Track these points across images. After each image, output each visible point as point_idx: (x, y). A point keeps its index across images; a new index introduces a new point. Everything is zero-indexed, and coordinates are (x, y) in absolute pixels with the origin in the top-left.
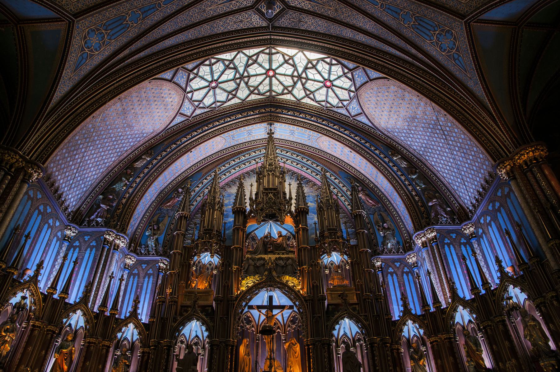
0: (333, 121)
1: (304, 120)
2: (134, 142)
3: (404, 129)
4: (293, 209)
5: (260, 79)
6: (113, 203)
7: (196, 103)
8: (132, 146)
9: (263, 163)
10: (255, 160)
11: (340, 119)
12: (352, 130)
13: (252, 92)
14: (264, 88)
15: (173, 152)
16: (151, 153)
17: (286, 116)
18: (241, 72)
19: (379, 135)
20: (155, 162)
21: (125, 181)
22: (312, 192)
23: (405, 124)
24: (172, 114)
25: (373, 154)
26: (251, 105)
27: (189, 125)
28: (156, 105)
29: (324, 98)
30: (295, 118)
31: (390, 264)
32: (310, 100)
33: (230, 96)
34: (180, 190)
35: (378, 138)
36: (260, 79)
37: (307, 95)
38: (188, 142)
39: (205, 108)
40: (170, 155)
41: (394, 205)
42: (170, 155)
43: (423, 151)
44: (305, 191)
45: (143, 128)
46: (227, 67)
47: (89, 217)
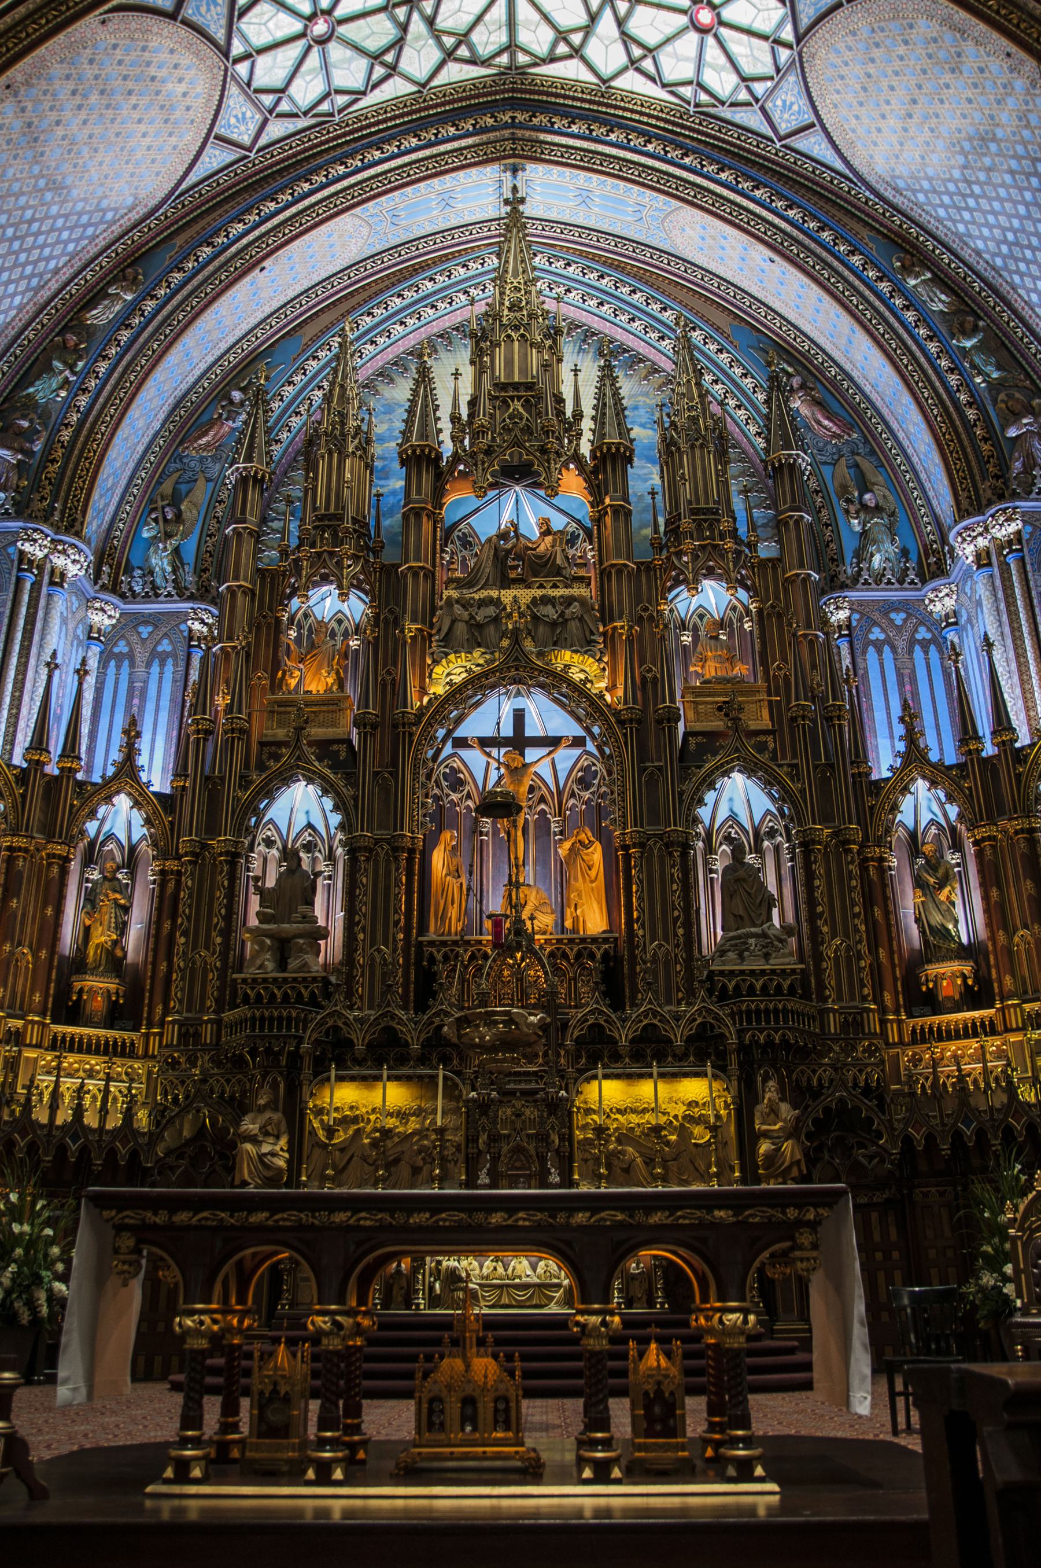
0: (716, 154)
1: (622, 154)
2: (77, 241)
3: (949, 180)
4: (585, 449)
6: (32, 442)
7: (268, 100)
8: (73, 255)
9: (490, 300)
10: (466, 292)
11: (740, 147)
12: (779, 187)
13: (449, 55)
15: (206, 272)
16: (135, 278)
17: (564, 140)
19: (866, 203)
20: (150, 305)
21: (62, 372)
22: (647, 395)
23: (953, 162)
24: (192, 139)
25: (841, 268)
26: (449, 103)
28: (135, 107)
29: (687, 71)
30: (593, 146)
31: (876, 616)
32: (642, 79)
33: (379, 71)
34: (237, 395)
38: (251, 237)
39: (296, 116)
40: (195, 282)
41: (901, 435)
42: (195, 282)
43: (1004, 257)
44: (623, 392)
45: (99, 193)
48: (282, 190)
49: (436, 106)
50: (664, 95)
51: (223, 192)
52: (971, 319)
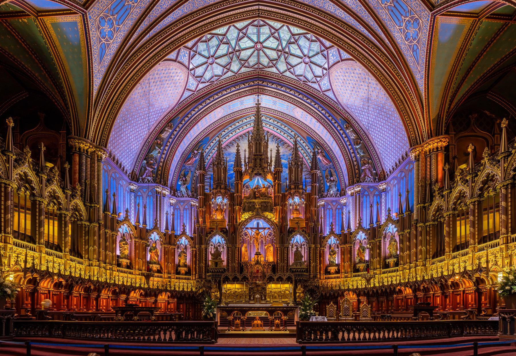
0: (306, 95)
1: (284, 93)
4: (272, 169)
5: (249, 52)
8: (156, 121)
11: (312, 93)
12: (321, 104)
13: (243, 65)
14: (252, 61)
17: (270, 89)
25: (332, 126)
27: (195, 99)
30: (277, 91)
33: (225, 70)
35: (339, 112)
36: (249, 52)
37: (288, 70)
38: (197, 115)
39: (205, 82)
40: (185, 126)
42: (185, 126)
45: (161, 105)
47: (142, 176)
48: (203, 102)
49: (240, 79)
50: (295, 78)
52: (359, 141)
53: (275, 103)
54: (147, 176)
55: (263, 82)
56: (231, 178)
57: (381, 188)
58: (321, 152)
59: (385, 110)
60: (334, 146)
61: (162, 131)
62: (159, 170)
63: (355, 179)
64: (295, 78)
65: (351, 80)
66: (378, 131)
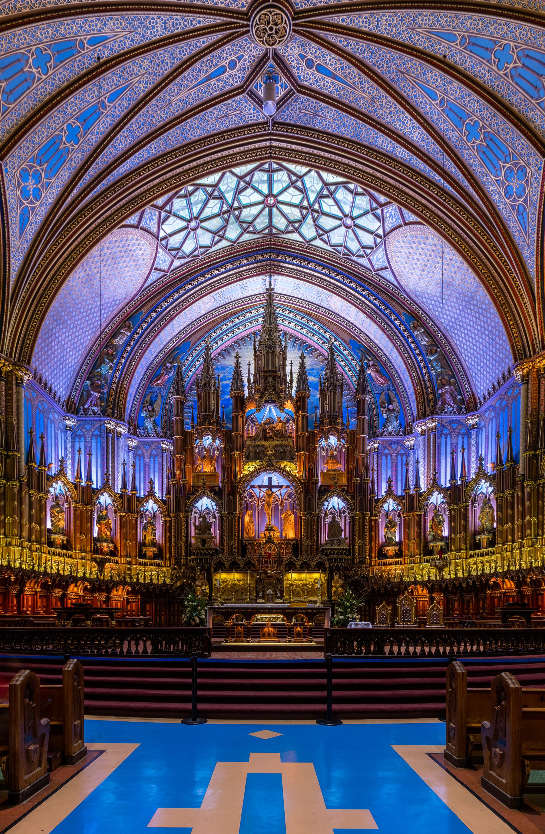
0: (349, 275)
1: (312, 273)
5: (255, 210)
13: (245, 230)
14: (261, 223)
15: (155, 323)
18: (230, 201)
20: (136, 337)
25: (391, 325)
30: (301, 269)
32: (322, 242)
33: (217, 238)
35: (402, 303)
36: (255, 210)
37: (319, 236)
38: (170, 308)
39: (184, 258)
40: (152, 326)
42: (152, 326)
46: (210, 196)
47: (83, 406)
48: (181, 288)
49: (240, 251)
50: (331, 249)
51: (158, 289)
52: (435, 348)
53: (298, 288)
54: (91, 405)
55: (278, 256)
56: (227, 406)
57: (470, 422)
58: (373, 365)
59: (475, 302)
60: (394, 356)
61: (115, 334)
62: (111, 396)
63: (428, 409)
64: (331, 249)
65: (420, 254)
66: (464, 333)
